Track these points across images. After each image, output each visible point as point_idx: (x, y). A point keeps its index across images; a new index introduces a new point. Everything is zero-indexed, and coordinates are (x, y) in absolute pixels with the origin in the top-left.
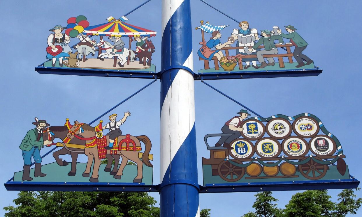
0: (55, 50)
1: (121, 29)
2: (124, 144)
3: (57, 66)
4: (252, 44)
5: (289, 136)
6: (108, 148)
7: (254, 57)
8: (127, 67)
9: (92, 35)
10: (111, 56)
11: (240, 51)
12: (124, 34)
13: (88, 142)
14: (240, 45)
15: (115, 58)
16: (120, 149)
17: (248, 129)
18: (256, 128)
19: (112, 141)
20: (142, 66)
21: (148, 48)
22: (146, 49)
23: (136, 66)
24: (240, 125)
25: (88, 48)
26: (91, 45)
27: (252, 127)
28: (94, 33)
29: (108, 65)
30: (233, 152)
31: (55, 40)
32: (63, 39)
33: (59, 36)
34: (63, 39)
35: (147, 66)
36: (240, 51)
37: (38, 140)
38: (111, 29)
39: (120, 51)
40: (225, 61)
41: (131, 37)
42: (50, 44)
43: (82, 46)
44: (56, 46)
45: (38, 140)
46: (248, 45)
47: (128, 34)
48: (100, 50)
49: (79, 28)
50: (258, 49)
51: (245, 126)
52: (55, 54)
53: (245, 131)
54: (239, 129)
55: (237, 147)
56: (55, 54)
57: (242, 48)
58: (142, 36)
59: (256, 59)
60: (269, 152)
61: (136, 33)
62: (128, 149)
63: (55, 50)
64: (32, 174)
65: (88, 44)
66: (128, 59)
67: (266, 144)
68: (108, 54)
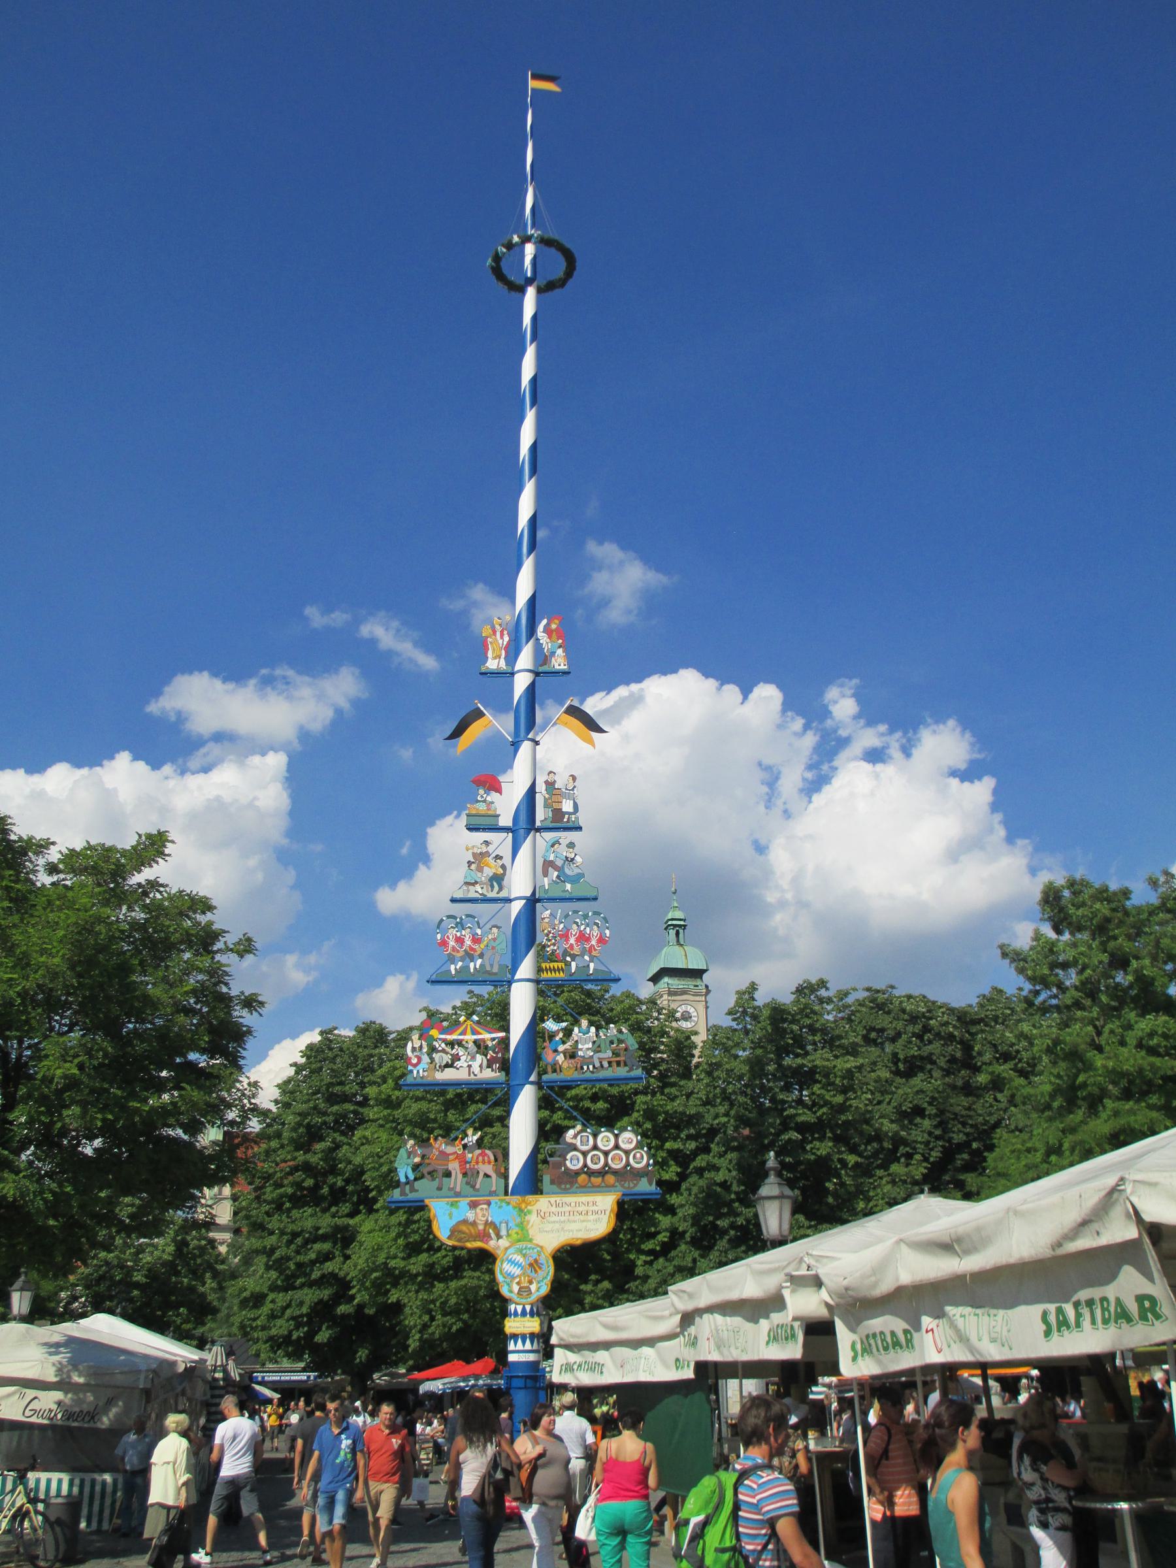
1: (474, 1032)
2: (480, 1159)
3: (419, 1081)
4: (590, 1045)
6: (466, 1162)
10: (465, 1065)
14: (580, 1046)
15: (470, 1066)
16: (477, 1163)
19: (470, 1156)
20: (493, 1075)
22: (497, 1053)
24: (575, 1136)
26: (447, 1053)
27: (585, 1139)
30: (568, 1163)
31: (414, 1049)
32: (421, 1047)
34: (421, 1047)
37: (409, 1157)
38: (464, 1033)
39: (473, 1058)
45: (409, 1157)
46: (587, 1046)
48: (456, 1058)
50: (596, 1052)
53: (578, 1144)
54: (574, 1141)
56: (415, 1065)
58: (493, 1039)
62: (484, 1162)
63: (415, 1061)
65: (443, 1051)
66: (481, 1066)
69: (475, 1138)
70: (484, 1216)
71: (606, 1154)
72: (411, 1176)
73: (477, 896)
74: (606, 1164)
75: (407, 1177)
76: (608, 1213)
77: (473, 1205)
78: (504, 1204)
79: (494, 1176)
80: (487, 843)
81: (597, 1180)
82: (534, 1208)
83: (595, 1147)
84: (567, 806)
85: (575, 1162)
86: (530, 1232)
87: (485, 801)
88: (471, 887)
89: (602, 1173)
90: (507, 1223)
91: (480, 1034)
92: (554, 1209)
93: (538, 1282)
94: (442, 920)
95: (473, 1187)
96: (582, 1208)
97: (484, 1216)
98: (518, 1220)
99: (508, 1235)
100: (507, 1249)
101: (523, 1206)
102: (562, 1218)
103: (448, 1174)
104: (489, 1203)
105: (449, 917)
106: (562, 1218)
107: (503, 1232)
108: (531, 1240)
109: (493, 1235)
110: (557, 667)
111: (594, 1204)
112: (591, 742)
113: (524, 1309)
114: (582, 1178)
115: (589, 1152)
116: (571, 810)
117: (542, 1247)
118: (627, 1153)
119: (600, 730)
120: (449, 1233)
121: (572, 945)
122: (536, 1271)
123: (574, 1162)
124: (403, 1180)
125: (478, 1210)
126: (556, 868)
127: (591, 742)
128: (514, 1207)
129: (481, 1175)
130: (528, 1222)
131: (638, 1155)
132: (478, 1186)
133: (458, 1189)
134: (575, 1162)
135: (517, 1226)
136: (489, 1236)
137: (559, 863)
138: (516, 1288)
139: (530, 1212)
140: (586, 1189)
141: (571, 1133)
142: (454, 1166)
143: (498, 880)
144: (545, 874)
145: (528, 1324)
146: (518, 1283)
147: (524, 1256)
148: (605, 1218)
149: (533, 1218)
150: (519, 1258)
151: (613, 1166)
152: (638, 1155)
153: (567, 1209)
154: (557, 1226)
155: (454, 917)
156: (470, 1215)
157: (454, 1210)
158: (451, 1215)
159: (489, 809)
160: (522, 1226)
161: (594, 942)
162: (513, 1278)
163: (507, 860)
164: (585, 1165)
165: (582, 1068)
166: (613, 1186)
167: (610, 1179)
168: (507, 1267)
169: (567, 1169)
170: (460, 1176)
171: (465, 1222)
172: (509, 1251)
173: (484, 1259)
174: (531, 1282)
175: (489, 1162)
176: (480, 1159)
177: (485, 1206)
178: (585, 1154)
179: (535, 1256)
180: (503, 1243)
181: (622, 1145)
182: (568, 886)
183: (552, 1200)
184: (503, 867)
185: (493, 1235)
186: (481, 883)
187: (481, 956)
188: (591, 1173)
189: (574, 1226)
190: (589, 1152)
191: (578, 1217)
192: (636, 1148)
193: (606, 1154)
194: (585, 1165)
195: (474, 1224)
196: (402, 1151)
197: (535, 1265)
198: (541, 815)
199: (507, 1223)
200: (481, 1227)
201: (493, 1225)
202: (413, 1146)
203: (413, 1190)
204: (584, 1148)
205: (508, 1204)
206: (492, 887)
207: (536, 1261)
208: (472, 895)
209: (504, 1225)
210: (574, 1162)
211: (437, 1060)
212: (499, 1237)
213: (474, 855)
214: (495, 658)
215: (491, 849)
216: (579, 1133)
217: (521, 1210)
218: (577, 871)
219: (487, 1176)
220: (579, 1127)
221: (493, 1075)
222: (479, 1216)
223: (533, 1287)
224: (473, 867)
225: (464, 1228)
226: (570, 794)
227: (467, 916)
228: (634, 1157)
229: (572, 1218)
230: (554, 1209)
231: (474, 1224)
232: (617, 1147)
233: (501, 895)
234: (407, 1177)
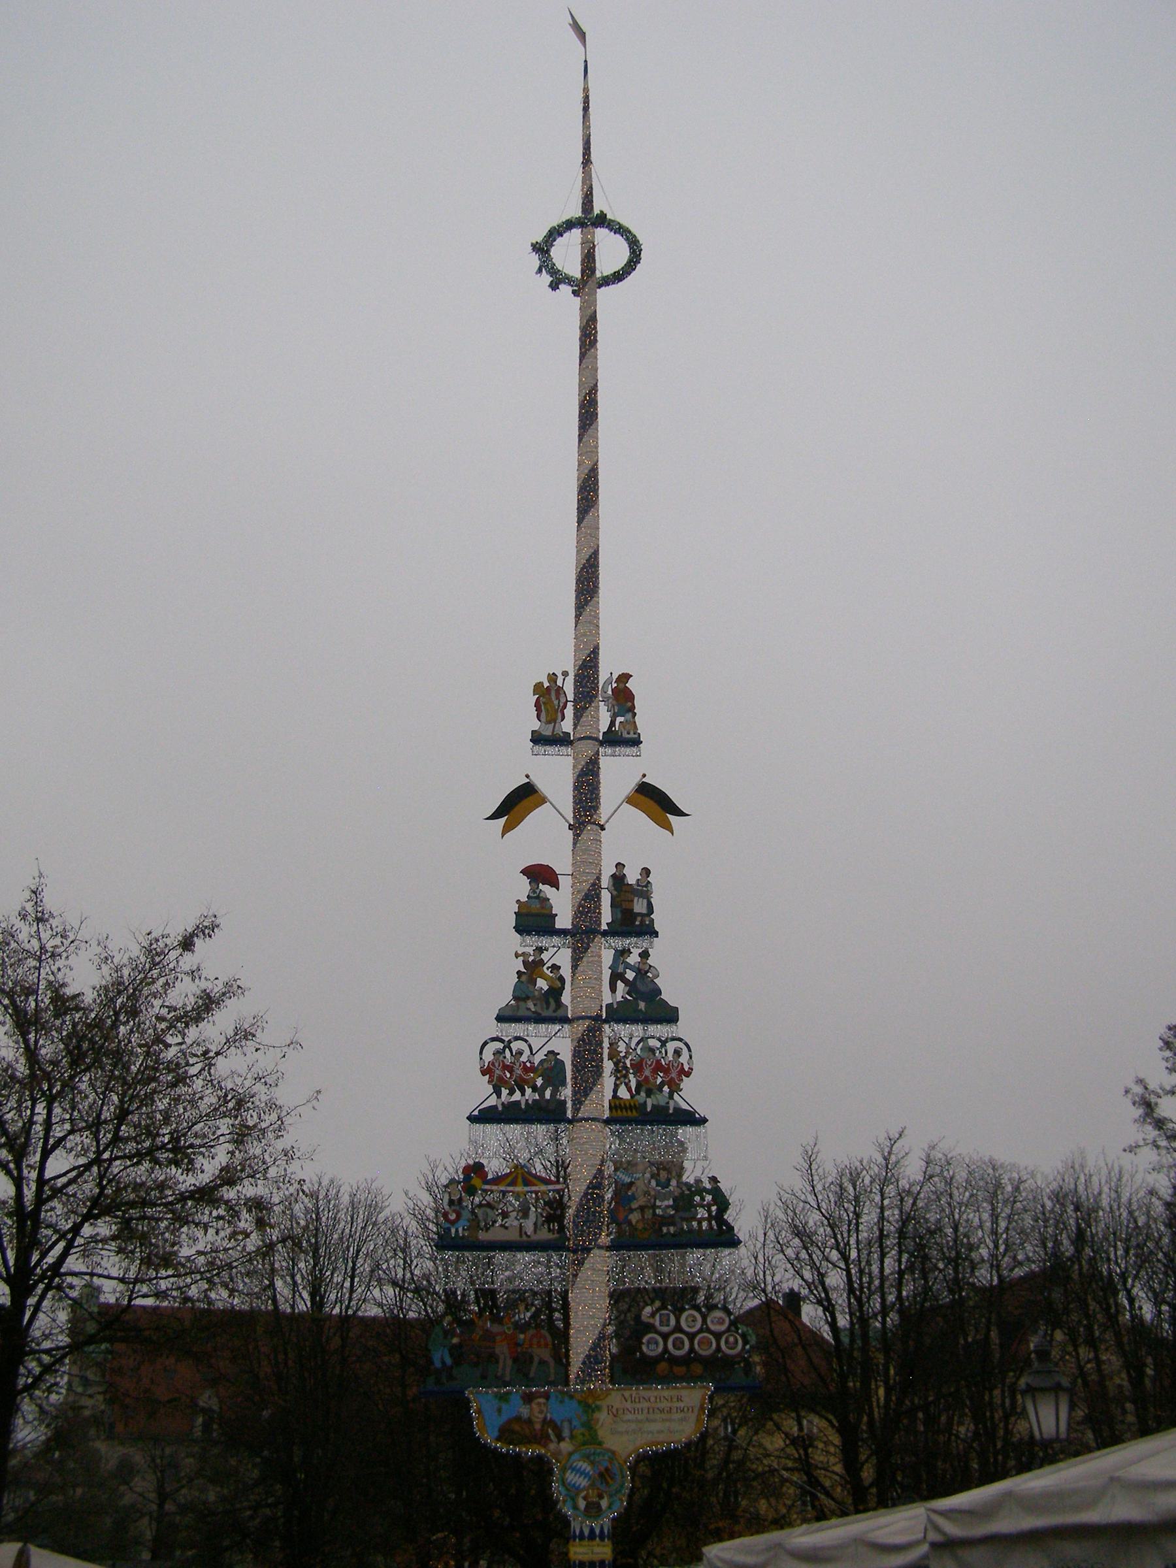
0: (453, 1217)
1: (527, 1183)
2: (535, 1341)
4: (671, 1202)
5: (701, 1331)
6: (517, 1344)
7: (670, 1221)
8: (535, 1238)
9: (492, 1192)
10: (516, 1223)
11: (658, 1211)
12: (526, 1189)
13: (498, 1338)
16: (531, 1345)
17: (661, 1321)
18: (668, 1320)
19: (522, 1336)
21: (555, 1210)
22: (555, 1210)
23: (544, 1235)
24: (653, 1315)
25: (488, 1210)
28: (494, 1188)
29: (512, 1236)
30: (644, 1348)
33: (455, 1198)
35: (556, 1236)
36: (658, 1211)
37: (445, 1337)
39: (526, 1215)
40: (640, 1226)
41: (536, 1193)
42: (447, 1207)
43: (483, 1209)
44: (454, 1211)
45: (445, 1337)
46: (666, 1203)
47: (534, 1188)
49: (476, 1181)
50: (677, 1211)
51: (657, 1316)
52: (453, 1223)
53: (657, 1324)
54: (651, 1321)
55: (649, 1342)
56: (453, 1223)
57: (659, 1207)
59: (673, 1224)
60: (679, 1349)
61: (543, 1188)
62: (539, 1345)
63: (453, 1217)
64: (444, 1379)
66: (535, 1224)
67: (676, 1338)
68: (512, 1222)
69: (528, 1314)
70: (541, 1412)
71: (691, 1337)
72: (449, 1361)
73: (528, 1014)
74: (692, 1349)
75: (443, 1362)
76: (696, 1410)
77: (528, 1398)
78: (567, 1399)
79: (552, 1362)
80: (540, 950)
81: (680, 1370)
82: (604, 1404)
83: (678, 1329)
84: (639, 907)
85: (652, 1346)
86: (601, 1433)
87: (538, 897)
88: (522, 1004)
89: (691, 1358)
90: (570, 1421)
91: (534, 1185)
92: (629, 1405)
93: (611, 1496)
94: (485, 1044)
95: (526, 1375)
96: (664, 1405)
97: (541, 1412)
98: (585, 1418)
99: (572, 1437)
100: (570, 1454)
101: (590, 1401)
102: (640, 1417)
103: (493, 1358)
104: (547, 1396)
105: (493, 1039)
106: (640, 1417)
107: (566, 1433)
108: (600, 1444)
109: (553, 1437)
110: (625, 735)
111: (679, 1399)
112: (668, 827)
113: (592, 1530)
114: (663, 1366)
115: (672, 1332)
116: (644, 911)
117: (613, 1453)
118: (718, 1336)
119: (679, 813)
120: (496, 1434)
121: (646, 1077)
122: (607, 1483)
123: (651, 1347)
124: (438, 1364)
125: (534, 1406)
126: (625, 981)
127: (668, 827)
128: (580, 1402)
129: (536, 1360)
130: (598, 1420)
131: (731, 1339)
132: (532, 1375)
133: (507, 1379)
134: (652, 1346)
135: (583, 1425)
136: (548, 1437)
137: (630, 975)
138: (582, 1504)
139: (599, 1408)
140: (667, 1379)
141: (648, 1309)
142: (502, 1349)
143: (555, 992)
144: (613, 989)
145: (597, 1550)
146: (585, 1498)
147: (592, 1463)
148: (693, 1417)
149: (603, 1416)
150: (585, 1466)
151: (701, 1352)
152: (731, 1339)
153: (645, 1405)
154: (633, 1426)
155: (502, 1041)
156: (525, 1411)
157: (505, 1406)
158: (499, 1410)
159: (543, 908)
160: (589, 1426)
161: (674, 1075)
162: (578, 1490)
163: (566, 972)
164: (666, 1350)
165: (661, 1230)
166: (701, 1378)
167: (698, 1369)
168: (570, 1477)
169: (642, 1352)
170: (509, 1362)
171: (518, 1419)
172: (574, 1457)
173: (542, 1469)
174: (601, 1497)
175: (546, 1345)
176: (535, 1341)
177: (542, 1400)
178: (665, 1337)
179: (606, 1464)
180: (566, 1446)
181: (712, 1327)
182: (642, 1005)
183: (627, 1394)
184: (562, 980)
185: (553, 1437)
186: (534, 998)
187: (535, 1089)
188: (674, 1361)
189: (654, 1427)
190: (672, 1332)
191: (658, 1416)
192: (728, 1330)
193: (691, 1337)
194: (666, 1350)
195: (529, 1421)
196: (437, 1329)
197: (605, 1476)
198: (606, 916)
199: (570, 1421)
200: (538, 1426)
201: (551, 1423)
202: (450, 1324)
203: (451, 1377)
204: (665, 1329)
205: (571, 1397)
206: (548, 1004)
207: (607, 1469)
208: (521, 1013)
209: (566, 1424)
210: (651, 1347)
211: (480, 1217)
212: (560, 1439)
213: (525, 963)
214: (549, 722)
215: (545, 956)
216: (658, 1310)
217: (588, 1406)
218: (651, 986)
219: (542, 1362)
220: (658, 1304)
221: (550, 1236)
222: (535, 1412)
223: (604, 1503)
224: (524, 978)
225: (517, 1427)
226: (643, 890)
227: (517, 1038)
228: (727, 1341)
229: (651, 1416)
230: (629, 1405)
231: (529, 1421)
232: (705, 1329)
233: (560, 1013)
234: (443, 1362)
